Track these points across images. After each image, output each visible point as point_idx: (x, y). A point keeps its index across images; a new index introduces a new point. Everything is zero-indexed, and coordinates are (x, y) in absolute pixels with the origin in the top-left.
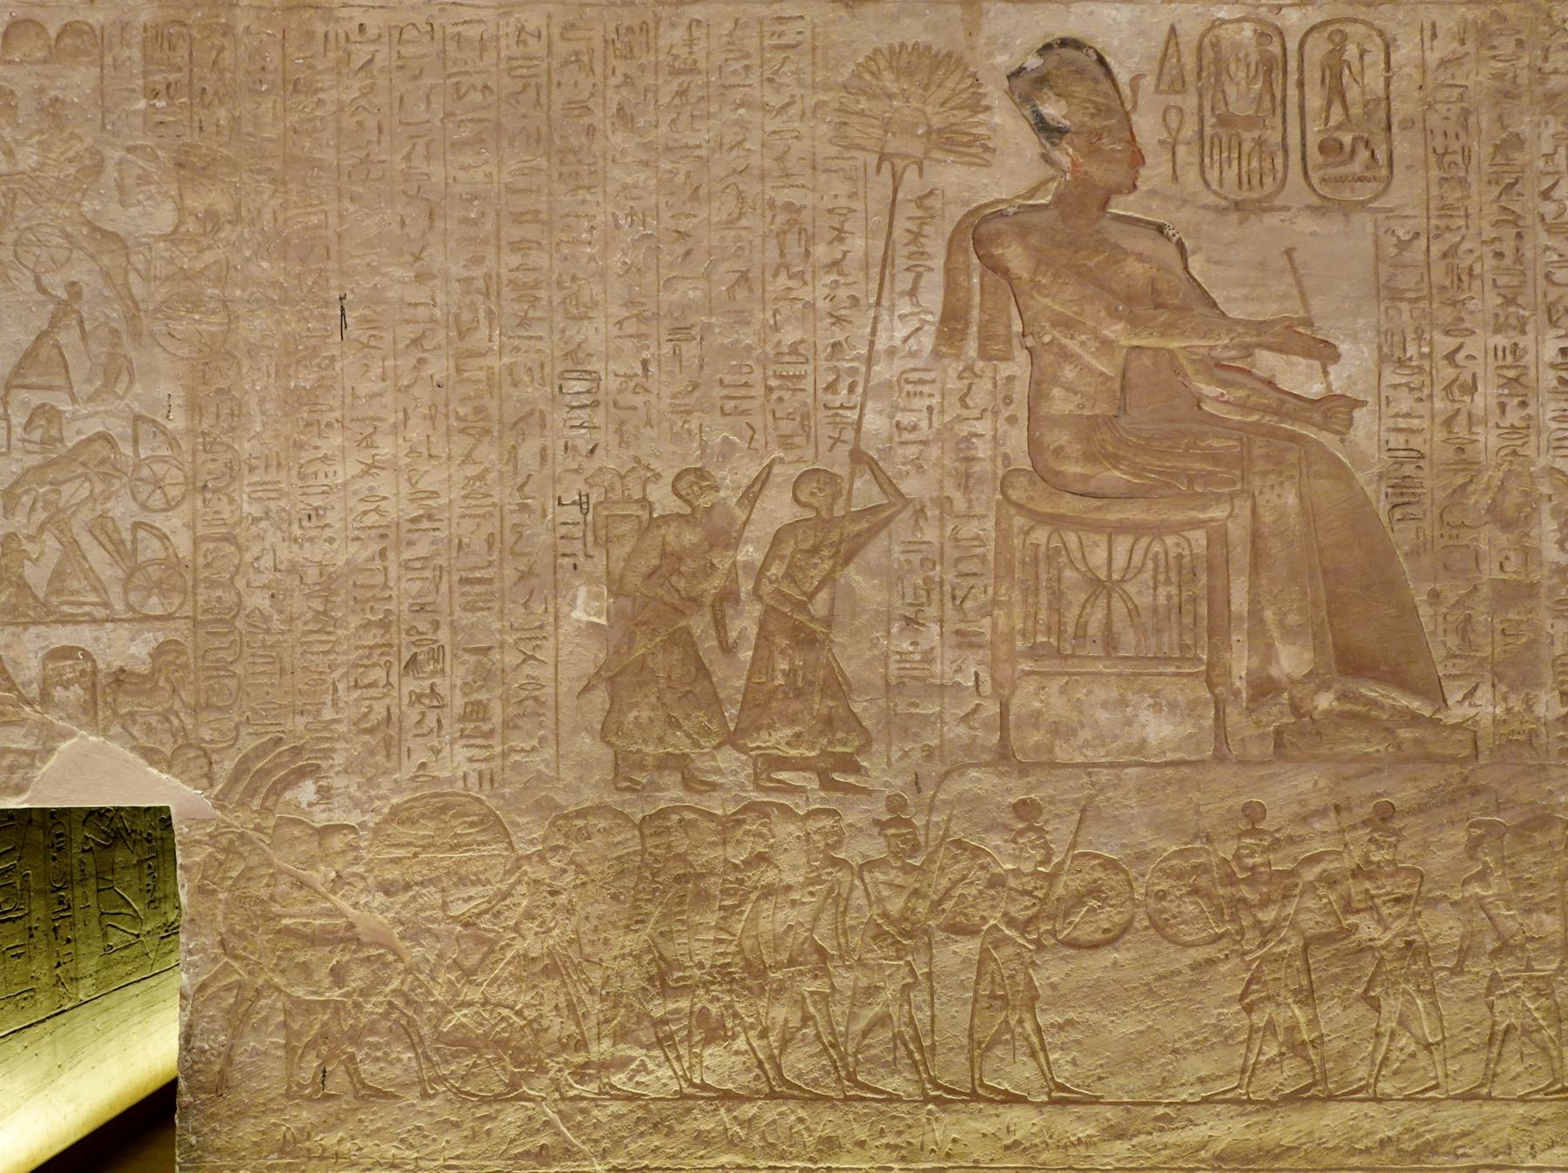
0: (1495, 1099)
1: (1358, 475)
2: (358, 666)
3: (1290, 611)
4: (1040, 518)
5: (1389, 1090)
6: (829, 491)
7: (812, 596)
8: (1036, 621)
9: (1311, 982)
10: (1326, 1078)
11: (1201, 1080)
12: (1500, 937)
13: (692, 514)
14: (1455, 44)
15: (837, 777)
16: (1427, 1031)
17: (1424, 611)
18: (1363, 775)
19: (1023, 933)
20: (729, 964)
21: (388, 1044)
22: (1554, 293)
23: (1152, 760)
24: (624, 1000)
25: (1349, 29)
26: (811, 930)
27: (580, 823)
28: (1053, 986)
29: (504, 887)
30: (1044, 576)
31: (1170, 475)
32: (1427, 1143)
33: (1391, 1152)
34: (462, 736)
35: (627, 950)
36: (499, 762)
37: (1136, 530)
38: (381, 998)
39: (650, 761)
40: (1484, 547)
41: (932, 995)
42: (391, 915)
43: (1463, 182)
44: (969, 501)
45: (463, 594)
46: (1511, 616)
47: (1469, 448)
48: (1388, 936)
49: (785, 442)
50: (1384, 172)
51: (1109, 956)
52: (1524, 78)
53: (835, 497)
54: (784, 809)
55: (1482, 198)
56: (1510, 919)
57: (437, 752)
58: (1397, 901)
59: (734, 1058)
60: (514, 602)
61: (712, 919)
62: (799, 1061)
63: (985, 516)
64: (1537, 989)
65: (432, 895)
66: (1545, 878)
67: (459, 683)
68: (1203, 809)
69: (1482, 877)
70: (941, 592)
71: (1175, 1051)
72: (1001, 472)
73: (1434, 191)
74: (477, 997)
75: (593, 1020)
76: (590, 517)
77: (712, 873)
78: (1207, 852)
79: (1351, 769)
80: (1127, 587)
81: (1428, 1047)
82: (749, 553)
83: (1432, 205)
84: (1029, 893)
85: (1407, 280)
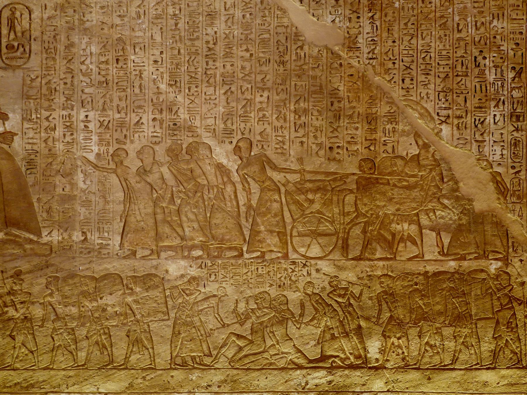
5: (19, 367)
12: (57, 315)
14: (53, 11)
17: (36, 204)
22: (84, 96)
25: (16, 6)
32: (31, 384)
33: (18, 387)
40: (58, 183)
43: (54, 59)
46: (66, 206)
47: (53, 149)
48: (18, 315)
50: (28, 55)
55: (61, 64)
56: (60, 309)
58: (22, 303)
69: (51, 295)
73: (44, 62)
81: (32, 352)
85: (33, 92)
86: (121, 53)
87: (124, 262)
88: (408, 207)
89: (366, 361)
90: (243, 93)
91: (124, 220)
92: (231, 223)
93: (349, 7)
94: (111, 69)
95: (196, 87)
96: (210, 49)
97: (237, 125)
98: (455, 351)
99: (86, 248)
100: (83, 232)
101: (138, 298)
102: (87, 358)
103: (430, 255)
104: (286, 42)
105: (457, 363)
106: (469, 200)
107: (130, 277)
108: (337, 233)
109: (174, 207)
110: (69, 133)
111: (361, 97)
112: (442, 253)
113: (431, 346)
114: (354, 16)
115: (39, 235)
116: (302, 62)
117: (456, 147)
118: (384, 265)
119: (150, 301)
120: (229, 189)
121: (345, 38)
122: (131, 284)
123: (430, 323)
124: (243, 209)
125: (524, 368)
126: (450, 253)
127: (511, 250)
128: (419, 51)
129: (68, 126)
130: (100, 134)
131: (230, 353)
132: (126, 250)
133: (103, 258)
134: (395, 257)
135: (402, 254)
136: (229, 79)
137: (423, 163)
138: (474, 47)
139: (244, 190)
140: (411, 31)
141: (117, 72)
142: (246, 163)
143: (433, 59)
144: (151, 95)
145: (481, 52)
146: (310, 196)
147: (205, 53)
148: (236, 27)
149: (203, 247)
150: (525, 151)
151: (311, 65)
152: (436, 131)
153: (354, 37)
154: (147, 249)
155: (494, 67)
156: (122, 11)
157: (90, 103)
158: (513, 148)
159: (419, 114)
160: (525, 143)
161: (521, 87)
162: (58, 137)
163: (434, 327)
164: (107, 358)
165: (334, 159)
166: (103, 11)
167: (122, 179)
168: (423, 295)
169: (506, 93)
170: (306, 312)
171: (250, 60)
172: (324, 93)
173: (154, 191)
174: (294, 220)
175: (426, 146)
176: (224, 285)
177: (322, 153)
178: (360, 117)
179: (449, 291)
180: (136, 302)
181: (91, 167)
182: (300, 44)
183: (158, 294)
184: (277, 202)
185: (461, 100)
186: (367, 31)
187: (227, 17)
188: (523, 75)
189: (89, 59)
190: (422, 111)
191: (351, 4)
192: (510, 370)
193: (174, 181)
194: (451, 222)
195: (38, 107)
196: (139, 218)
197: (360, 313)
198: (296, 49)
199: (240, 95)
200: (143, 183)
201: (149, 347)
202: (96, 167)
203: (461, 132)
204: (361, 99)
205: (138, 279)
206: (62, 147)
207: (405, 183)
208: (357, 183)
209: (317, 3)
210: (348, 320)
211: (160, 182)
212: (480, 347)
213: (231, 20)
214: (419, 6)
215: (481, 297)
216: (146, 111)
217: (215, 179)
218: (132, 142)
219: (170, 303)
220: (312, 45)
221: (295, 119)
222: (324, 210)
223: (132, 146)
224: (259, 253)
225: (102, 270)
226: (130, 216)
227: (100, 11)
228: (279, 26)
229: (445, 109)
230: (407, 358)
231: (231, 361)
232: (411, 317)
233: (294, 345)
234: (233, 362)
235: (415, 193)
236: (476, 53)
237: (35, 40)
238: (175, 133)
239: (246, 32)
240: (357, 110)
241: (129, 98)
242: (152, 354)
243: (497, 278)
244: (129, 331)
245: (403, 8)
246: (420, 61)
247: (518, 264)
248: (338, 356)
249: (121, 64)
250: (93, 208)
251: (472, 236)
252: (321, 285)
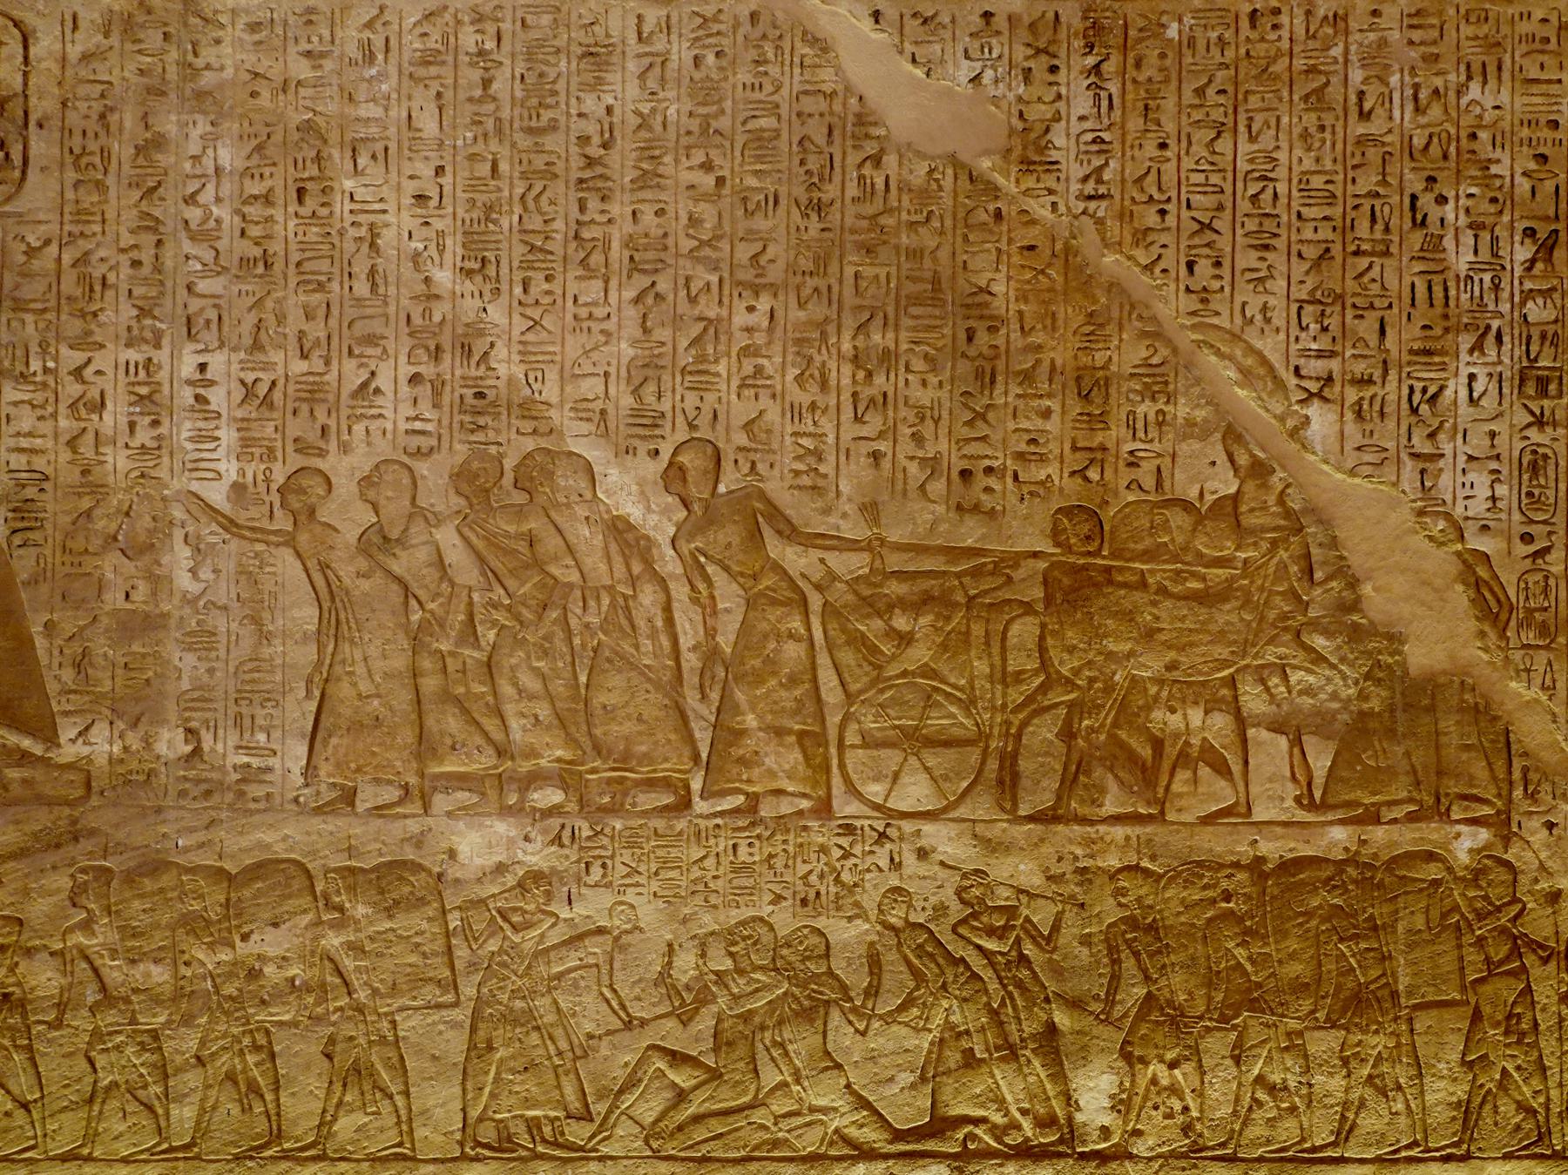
12: (103, 988)
17: (40, 643)
22: (195, 305)
40: (110, 575)
43: (100, 186)
46: (136, 647)
50: (17, 174)
52: (172, 73)
55: (122, 204)
56: (115, 972)
64: (141, 1043)
66: (156, 926)
69: (87, 926)
81: (25, 1106)
83: (67, 210)
86: (313, 171)
87: (317, 823)
88: (1204, 658)
89: (1072, 1133)
90: (693, 300)
91: (317, 693)
92: (651, 703)
93: (1023, 34)
94: (281, 219)
95: (548, 279)
96: (591, 162)
97: (675, 398)
98: (1346, 1105)
99: (198, 782)
100: (189, 731)
101: (361, 936)
102: (198, 1123)
103: (1272, 808)
104: (830, 143)
105: (1352, 1141)
106: (1391, 637)
107: (335, 870)
108: (982, 737)
109: (476, 654)
110: (147, 420)
111: (1061, 316)
112: (1306, 801)
113: (1272, 1089)
114: (1039, 65)
115: (52, 740)
116: (878, 204)
117: (1352, 472)
118: (1127, 838)
120: (648, 597)
121: (1012, 132)
122: (338, 893)
123: (1268, 1018)
124: (691, 661)
125: (1556, 1156)
126: (1331, 801)
127: (1518, 793)
128: (1240, 176)
129: (142, 397)
130: (243, 425)
131: (649, 1110)
133: (252, 813)
134: (1162, 812)
135: (1183, 803)
136: (650, 255)
137: (1250, 521)
138: (1408, 164)
139: (695, 601)
140: (1217, 115)
141: (300, 231)
142: (701, 517)
143: (1283, 200)
144: (405, 302)
145: (1431, 180)
146: (901, 622)
147: (575, 175)
148: (671, 94)
149: (566, 777)
150: (1562, 486)
151: (904, 216)
152: (1290, 423)
153: (1040, 128)
154: (389, 782)
155: (1470, 226)
156: (315, 39)
157: (214, 326)
158: (1526, 477)
159: (1241, 370)
160: (1562, 463)
161: (1553, 289)
162: (110, 433)
163: (1281, 1029)
164: (261, 1126)
165: (976, 508)
166: (257, 37)
167: (312, 564)
168: (1246, 932)
169: (1505, 307)
170: (887, 982)
171: (714, 197)
172: (945, 302)
173: (413, 602)
174: (849, 697)
175: (1260, 471)
176: (630, 897)
177: (938, 487)
178: (1057, 378)
179: (1328, 919)
180: (351, 947)
181: (214, 527)
182: (871, 148)
183: (425, 925)
184: (799, 640)
185: (1367, 328)
186: (1082, 112)
187: (646, 61)
188: (1559, 254)
189: (210, 188)
190: (1249, 361)
191: (1032, 26)
192: (1514, 1163)
193: (476, 572)
194: (1335, 705)
195: (51, 335)
196: (365, 687)
197: (1052, 987)
198: (860, 166)
199: (683, 307)
200: (379, 578)
201: (393, 1089)
202: (230, 525)
203: (1368, 427)
204: (1060, 323)
205: (361, 878)
206: (123, 464)
207: (1194, 585)
208: (1045, 583)
209: (925, 22)
210: (1015, 1008)
211: (432, 574)
212: (1422, 1092)
213: (657, 70)
214: (1242, 37)
215: (1426, 936)
216: (391, 352)
217: (603, 567)
218: (345, 448)
219: (462, 953)
220: (907, 151)
221: (854, 382)
222: (943, 667)
223: (347, 461)
224: (742, 798)
226: (339, 679)
227: (246, 37)
228: (806, 93)
229: (1320, 354)
230: (1198, 1127)
231: (651, 1133)
232: (1210, 999)
233: (848, 1086)
234: (658, 1136)
235: (1227, 615)
236: (1415, 183)
237: (41, 126)
238: (481, 421)
239: (702, 110)
240: (1046, 357)
241: (335, 311)
242: (403, 1112)
243: (1476, 879)
244: (332, 1040)
245: (1192, 43)
246: (1244, 206)
247: (1539, 837)
248: (984, 1120)
249: (311, 203)
250: (222, 653)
251: (1399, 750)
252: (933, 900)
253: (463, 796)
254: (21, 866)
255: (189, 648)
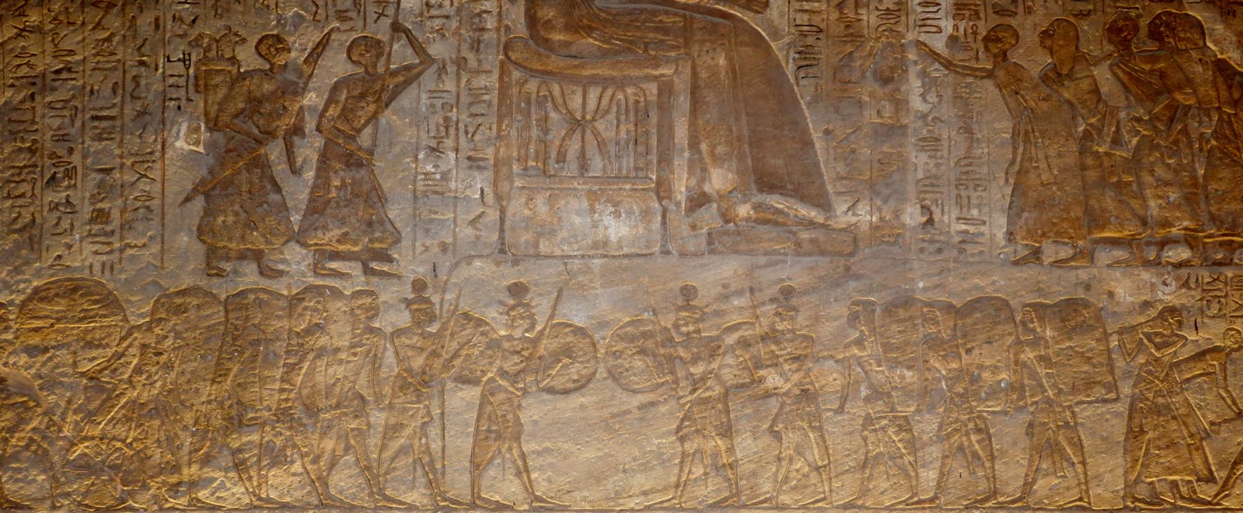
0: (868, 508)
1: (773, 44)
2: (9, 181)
3: (720, 143)
4: (532, 72)
6: (373, 52)
7: (359, 131)
8: (527, 149)
9: (729, 420)
10: (738, 494)
11: (645, 493)
13: (271, 70)
15: (375, 265)
16: (817, 457)
17: (818, 145)
18: (771, 265)
19: (513, 383)
20: (290, 408)
21: (27, 469)
23: (613, 253)
24: (210, 435)
26: (354, 382)
27: (178, 301)
28: (535, 422)
29: (120, 350)
30: (534, 117)
31: (631, 42)
34: (90, 235)
35: (213, 397)
36: (117, 255)
37: (605, 82)
38: (22, 435)
39: (233, 254)
41: (444, 429)
42: (33, 371)
44: (480, 61)
45: (95, 127)
46: (885, 149)
48: (788, 386)
49: (342, 16)
51: (577, 400)
53: (379, 56)
54: (331, 289)
56: (880, 373)
57: (69, 247)
59: (291, 479)
60: (131, 134)
61: (278, 373)
62: (341, 480)
63: (491, 72)
64: (900, 426)
65: (64, 356)
66: (907, 343)
67: (88, 195)
68: (650, 290)
69: (859, 343)
70: (457, 129)
71: (625, 471)
72: (503, 39)
74: (97, 432)
75: (186, 450)
76: (191, 71)
77: (278, 339)
78: (652, 322)
79: (763, 260)
80: (597, 124)
81: (818, 469)
82: (312, 99)
84: (518, 353)
87: (1018, 273)
91: (1012, 181)
100: (923, 207)
102: (939, 484)
119: (1077, 360)
132: (1019, 247)
149: (1190, 240)
154: (1065, 244)
164: (983, 486)
173: (1080, 119)
180: (1044, 359)
181: (937, 65)
183: (1093, 343)
206: (873, 20)
218: (1029, 11)
219: (1120, 363)
225: (969, 291)
226: (1027, 172)
244: (1031, 425)
250: (945, 153)
253: (1120, 254)
254: (813, 298)
255: (922, 149)
